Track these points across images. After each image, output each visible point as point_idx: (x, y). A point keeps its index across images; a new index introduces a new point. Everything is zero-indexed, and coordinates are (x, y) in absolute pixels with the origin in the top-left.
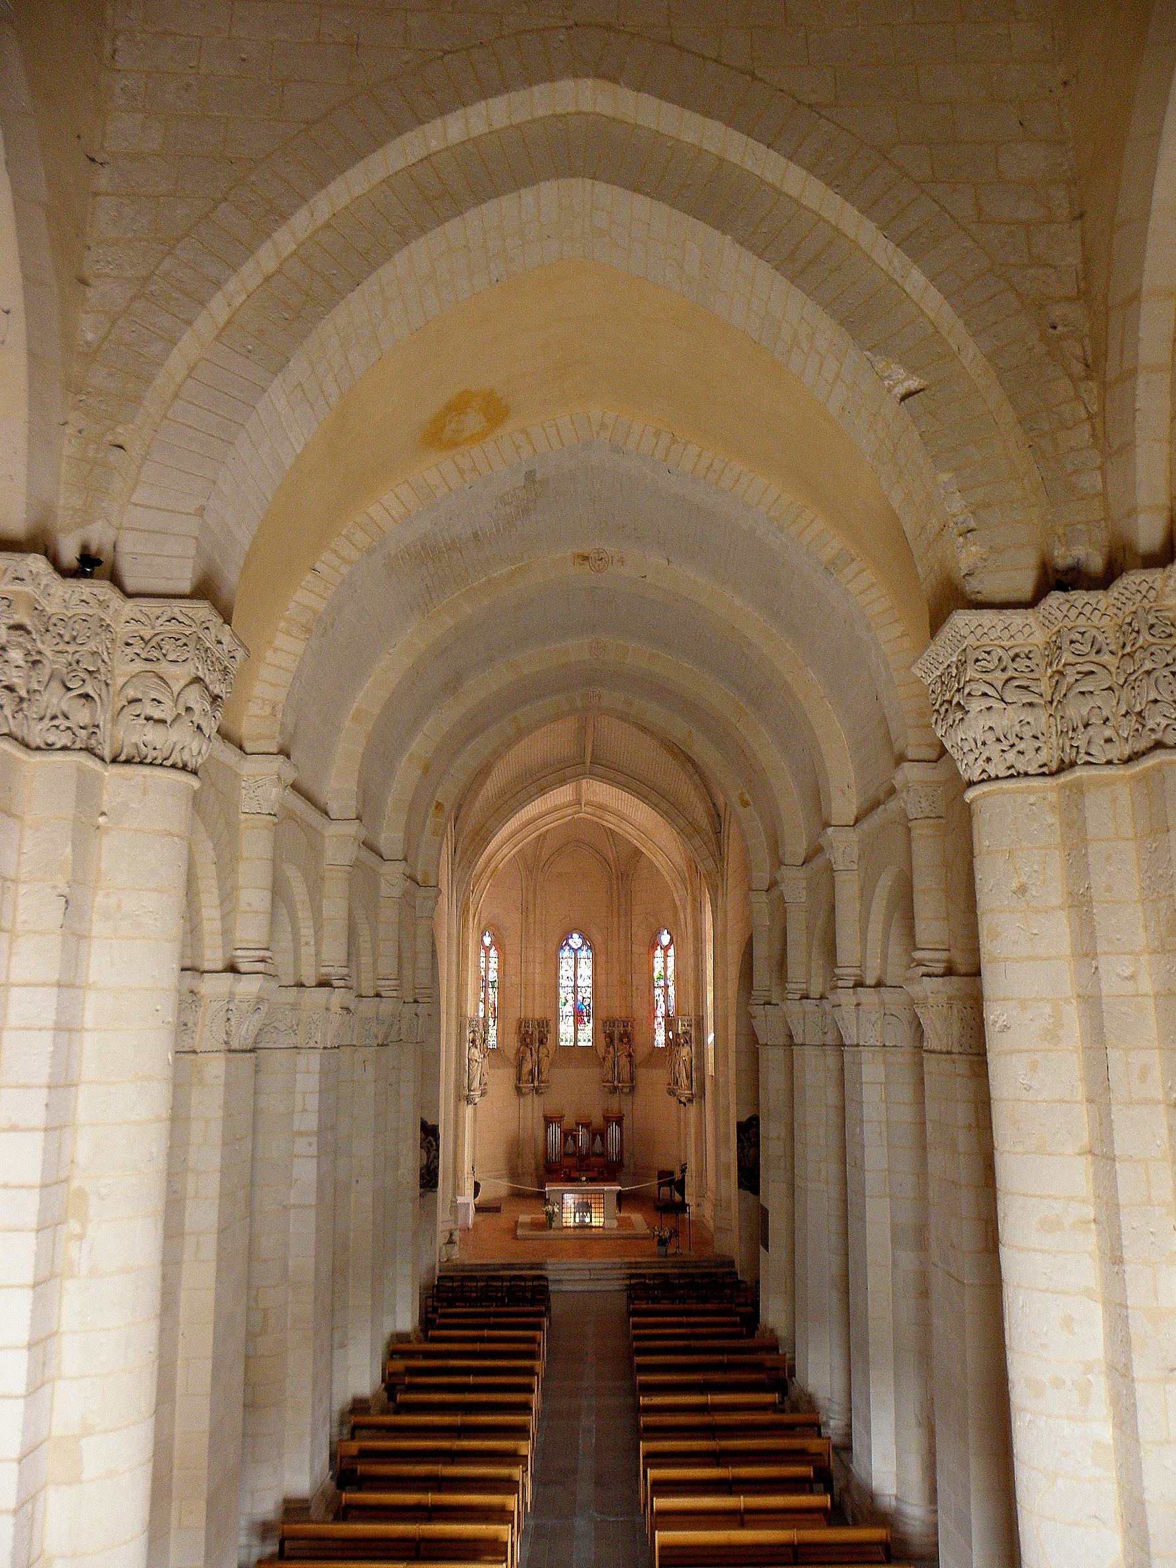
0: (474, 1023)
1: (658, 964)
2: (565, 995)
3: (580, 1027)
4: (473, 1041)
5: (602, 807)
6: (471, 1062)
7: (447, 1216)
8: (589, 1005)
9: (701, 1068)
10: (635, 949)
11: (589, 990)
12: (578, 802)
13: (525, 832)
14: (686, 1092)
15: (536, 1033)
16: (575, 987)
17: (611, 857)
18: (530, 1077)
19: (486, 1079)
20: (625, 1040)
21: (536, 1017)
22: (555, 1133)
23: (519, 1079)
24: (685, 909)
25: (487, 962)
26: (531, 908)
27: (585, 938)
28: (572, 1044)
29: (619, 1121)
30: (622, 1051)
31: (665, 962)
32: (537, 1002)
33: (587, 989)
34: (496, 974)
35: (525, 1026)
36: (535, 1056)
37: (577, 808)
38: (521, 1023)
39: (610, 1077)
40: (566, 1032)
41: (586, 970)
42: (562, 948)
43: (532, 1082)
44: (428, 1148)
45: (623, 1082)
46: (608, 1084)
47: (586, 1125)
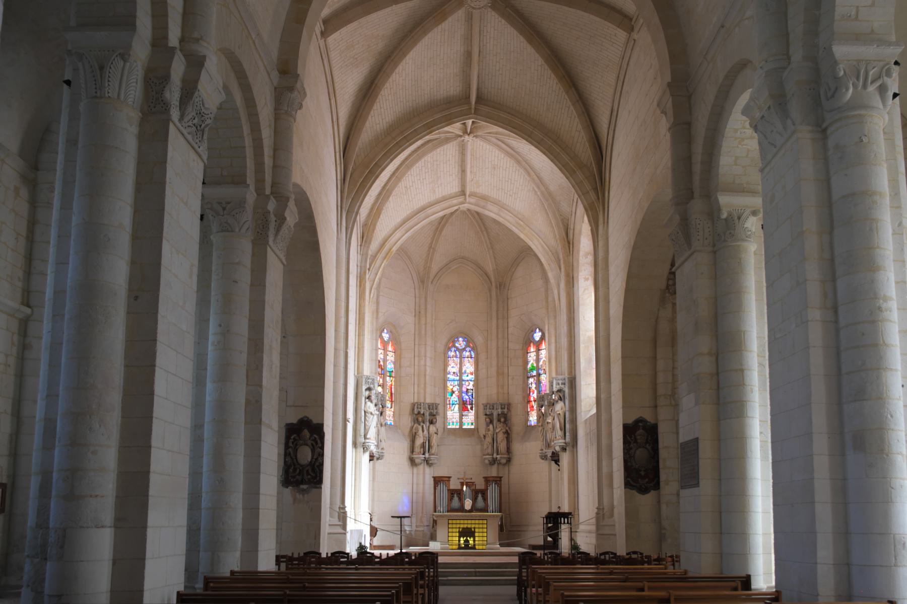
0: (370, 381)
1: (532, 357)
2: (451, 387)
3: (465, 413)
4: (369, 398)
6: (367, 414)
7: (336, 521)
8: (473, 395)
9: (574, 421)
10: (511, 346)
11: (472, 383)
13: (415, 220)
14: (560, 441)
15: (427, 414)
16: (461, 380)
17: (490, 267)
18: (422, 449)
20: (502, 420)
21: (428, 401)
22: (443, 491)
23: (412, 450)
24: (558, 285)
25: (386, 355)
26: (423, 312)
27: (469, 341)
28: (458, 427)
29: (498, 480)
30: (500, 428)
32: (429, 390)
33: (470, 382)
34: (393, 366)
35: (418, 408)
38: (414, 405)
39: (490, 451)
40: (453, 415)
41: (469, 367)
42: (449, 349)
43: (424, 454)
44: (312, 445)
45: (502, 454)
46: (487, 456)
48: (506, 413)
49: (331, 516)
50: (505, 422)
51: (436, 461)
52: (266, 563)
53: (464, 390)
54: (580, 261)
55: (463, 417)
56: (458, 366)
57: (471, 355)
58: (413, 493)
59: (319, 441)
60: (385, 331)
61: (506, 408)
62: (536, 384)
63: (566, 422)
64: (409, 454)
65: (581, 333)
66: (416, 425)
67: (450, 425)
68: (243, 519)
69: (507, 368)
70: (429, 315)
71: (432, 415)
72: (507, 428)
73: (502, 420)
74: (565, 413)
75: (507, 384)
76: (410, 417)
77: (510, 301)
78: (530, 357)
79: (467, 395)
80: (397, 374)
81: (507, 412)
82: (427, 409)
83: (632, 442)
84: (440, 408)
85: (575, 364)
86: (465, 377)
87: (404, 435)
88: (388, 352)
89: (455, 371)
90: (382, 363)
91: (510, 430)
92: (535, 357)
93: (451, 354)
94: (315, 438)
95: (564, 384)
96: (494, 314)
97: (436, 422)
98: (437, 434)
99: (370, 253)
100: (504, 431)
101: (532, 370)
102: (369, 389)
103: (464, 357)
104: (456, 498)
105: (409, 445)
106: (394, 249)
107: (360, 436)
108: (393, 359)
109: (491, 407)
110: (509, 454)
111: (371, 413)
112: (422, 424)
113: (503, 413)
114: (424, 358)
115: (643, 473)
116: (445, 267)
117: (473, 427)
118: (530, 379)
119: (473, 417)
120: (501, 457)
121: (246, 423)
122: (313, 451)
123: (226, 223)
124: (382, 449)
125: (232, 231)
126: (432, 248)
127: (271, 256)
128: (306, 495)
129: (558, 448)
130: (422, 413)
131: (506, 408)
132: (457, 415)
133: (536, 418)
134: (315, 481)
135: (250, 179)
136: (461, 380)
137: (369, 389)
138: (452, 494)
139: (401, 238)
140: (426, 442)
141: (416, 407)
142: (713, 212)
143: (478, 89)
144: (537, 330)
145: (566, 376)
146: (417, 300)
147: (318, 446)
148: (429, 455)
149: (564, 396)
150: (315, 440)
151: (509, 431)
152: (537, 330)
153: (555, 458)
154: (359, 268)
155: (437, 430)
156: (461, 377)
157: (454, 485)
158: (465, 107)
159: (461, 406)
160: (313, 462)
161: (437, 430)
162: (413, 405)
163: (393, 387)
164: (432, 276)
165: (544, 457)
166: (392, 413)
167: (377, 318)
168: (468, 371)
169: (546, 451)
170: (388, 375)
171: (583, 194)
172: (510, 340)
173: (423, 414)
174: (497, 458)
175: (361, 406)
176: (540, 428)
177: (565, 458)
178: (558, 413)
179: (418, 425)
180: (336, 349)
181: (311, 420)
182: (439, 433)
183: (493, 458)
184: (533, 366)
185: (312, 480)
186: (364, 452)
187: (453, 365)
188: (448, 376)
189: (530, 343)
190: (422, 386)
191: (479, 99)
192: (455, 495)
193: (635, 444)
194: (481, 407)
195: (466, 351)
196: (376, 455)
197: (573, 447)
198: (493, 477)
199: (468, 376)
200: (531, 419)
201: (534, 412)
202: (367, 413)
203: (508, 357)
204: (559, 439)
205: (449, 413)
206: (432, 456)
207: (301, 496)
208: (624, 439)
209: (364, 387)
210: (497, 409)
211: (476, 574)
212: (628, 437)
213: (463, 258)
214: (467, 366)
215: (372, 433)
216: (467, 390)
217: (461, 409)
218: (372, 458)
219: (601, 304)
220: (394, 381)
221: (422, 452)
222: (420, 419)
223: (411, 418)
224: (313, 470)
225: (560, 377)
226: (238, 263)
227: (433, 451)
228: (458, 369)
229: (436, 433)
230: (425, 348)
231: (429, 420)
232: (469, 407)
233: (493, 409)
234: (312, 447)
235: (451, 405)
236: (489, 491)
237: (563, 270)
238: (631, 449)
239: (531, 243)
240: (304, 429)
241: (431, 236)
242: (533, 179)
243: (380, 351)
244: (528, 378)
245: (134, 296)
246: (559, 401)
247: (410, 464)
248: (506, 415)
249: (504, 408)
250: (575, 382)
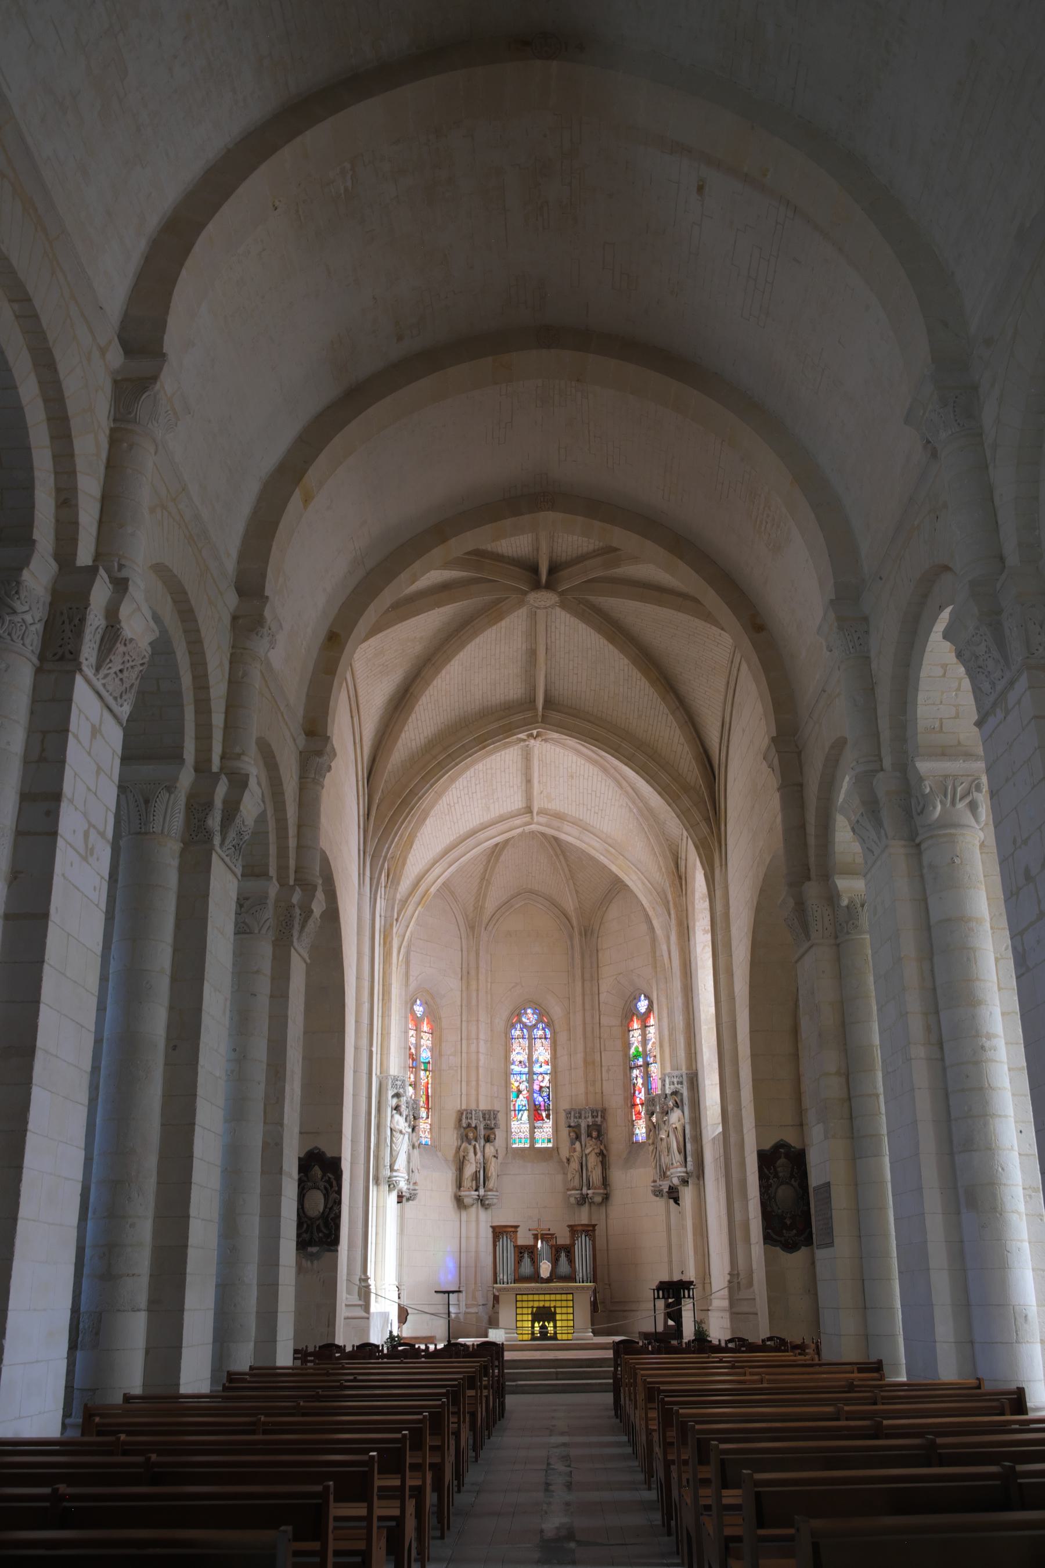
0: (399, 1083)
1: (635, 1037)
2: (517, 1084)
3: (538, 1124)
4: (397, 1108)
5: (560, 816)
6: (394, 1133)
7: (355, 1299)
8: (549, 1095)
9: (698, 1138)
10: (604, 1021)
11: (547, 1077)
12: (529, 810)
14: (679, 1169)
15: (481, 1127)
16: (531, 1073)
17: (570, 904)
18: (474, 1182)
19: (416, 1177)
20: (594, 1134)
21: (483, 1106)
22: (507, 1247)
23: (459, 1185)
24: (668, 938)
25: (419, 1038)
26: (473, 972)
27: (542, 1014)
28: (527, 1146)
30: (591, 1148)
31: (644, 1035)
32: (483, 1090)
33: (545, 1076)
34: (429, 1054)
35: (467, 1118)
36: (479, 1154)
37: (526, 818)
38: (462, 1114)
39: (576, 1182)
40: (520, 1126)
41: (543, 1053)
42: (513, 1026)
44: (326, 1188)
45: (595, 1188)
46: (573, 1192)
47: (546, 1237)
48: (599, 1123)
49: (349, 1292)
50: (598, 1137)
51: (495, 1201)
52: (284, 1358)
53: (536, 1087)
54: (696, 906)
55: (536, 1130)
56: (527, 1051)
57: (545, 1035)
58: (460, 1252)
59: (334, 1183)
60: (418, 1002)
61: (599, 1117)
62: (643, 1078)
63: (687, 1140)
64: (455, 1190)
65: (701, 1008)
66: (464, 1145)
67: (515, 1143)
68: (257, 1299)
69: (599, 1053)
70: (482, 977)
71: (487, 1127)
72: (602, 1147)
73: (594, 1134)
74: (684, 1127)
75: (600, 1078)
76: (456, 1132)
77: (600, 955)
78: (633, 1036)
79: (540, 1096)
80: (435, 1067)
81: (602, 1122)
82: (481, 1119)
83: (772, 1176)
84: (501, 1117)
85: (696, 1053)
86: (536, 1069)
87: (446, 1160)
88: (422, 1034)
89: (522, 1059)
90: (413, 1051)
91: (607, 1150)
92: (640, 1037)
93: (516, 1033)
94: (329, 1178)
95: (681, 1083)
96: (578, 973)
97: (495, 1139)
98: (497, 1158)
99: (398, 896)
100: (597, 1151)
101: (636, 1057)
102: (397, 1095)
103: (535, 1038)
104: (527, 1260)
105: (454, 1178)
106: (433, 890)
107: (385, 1166)
108: (429, 1043)
109: (577, 1115)
110: (605, 1188)
111: (401, 1132)
112: (473, 1143)
113: (595, 1124)
114: (475, 1041)
115: (788, 1222)
116: (506, 904)
117: (550, 1145)
118: (635, 1071)
119: (551, 1130)
120: (593, 1193)
121: (263, 1172)
122: (326, 1196)
123: (244, 922)
124: (415, 1184)
125: (250, 933)
126: (485, 880)
127: (295, 958)
128: (315, 1262)
129: (676, 1181)
130: (473, 1125)
131: (599, 1117)
132: (526, 1127)
133: (644, 1130)
134: (329, 1240)
135: (272, 872)
136: (531, 1073)
137: (397, 1095)
138: (521, 1253)
139: (441, 874)
140: (479, 1171)
141: (464, 1116)
142: (832, 897)
143: (546, 691)
144: (642, 997)
145: (684, 1071)
146: (465, 953)
147: (333, 1189)
148: (485, 1191)
149: (682, 1100)
150: (329, 1182)
151: (605, 1152)
152: (642, 997)
153: (674, 1195)
154: (383, 918)
155: (497, 1151)
156: (531, 1068)
157: (524, 1238)
158: (530, 714)
159: (532, 1112)
160: (326, 1214)
161: (497, 1151)
162: (460, 1113)
163: (430, 1086)
164: (485, 921)
165: (658, 1193)
166: (429, 1127)
167: (407, 985)
168: (541, 1059)
169: (661, 1183)
170: (423, 1068)
171: (690, 825)
172: (602, 1012)
173: (476, 1128)
174: (587, 1194)
175: (386, 1120)
176: (651, 1148)
177: (687, 1195)
178: (674, 1126)
179: (467, 1145)
180: (356, 1048)
181: (323, 1153)
182: (500, 1157)
183: (582, 1194)
184: (638, 1051)
185: (324, 1240)
186: (390, 1190)
187: (518, 1049)
188: (512, 1067)
189: (633, 1014)
190: (474, 1083)
191: (549, 702)
192: (526, 1255)
193: (775, 1179)
194: (562, 1116)
195: (538, 1029)
196: (406, 1194)
197: (698, 1178)
198: (582, 1225)
199: (541, 1066)
200: (637, 1131)
201: (642, 1121)
202: (395, 1131)
203: (600, 1038)
204: (677, 1168)
205: (514, 1125)
206: (489, 1193)
207: (309, 1263)
208: (759, 1171)
209: (390, 1093)
210: (585, 1118)
211: (557, 1376)
212: (766, 1170)
213: (532, 892)
214: (539, 1051)
215: (401, 1163)
216: (541, 1087)
217: (532, 1117)
218: (400, 1198)
219: (722, 977)
220: (432, 1077)
221: (474, 1188)
222: (471, 1135)
223: (457, 1134)
224: (327, 1225)
225: (676, 1073)
226: (257, 972)
227: (491, 1184)
228: (526, 1057)
229: (495, 1156)
230: (478, 1028)
231: (484, 1136)
232: (544, 1114)
233: (580, 1117)
234: (324, 1192)
236: (576, 1246)
237: (673, 916)
238: (771, 1185)
239: (626, 877)
240: (314, 1166)
241: (484, 864)
242: (627, 792)
243: (412, 1033)
244: (631, 1068)
245: (172, 1047)
246: (675, 1109)
247: (456, 1206)
248: (600, 1126)
249: (597, 1117)
250: (697, 1080)
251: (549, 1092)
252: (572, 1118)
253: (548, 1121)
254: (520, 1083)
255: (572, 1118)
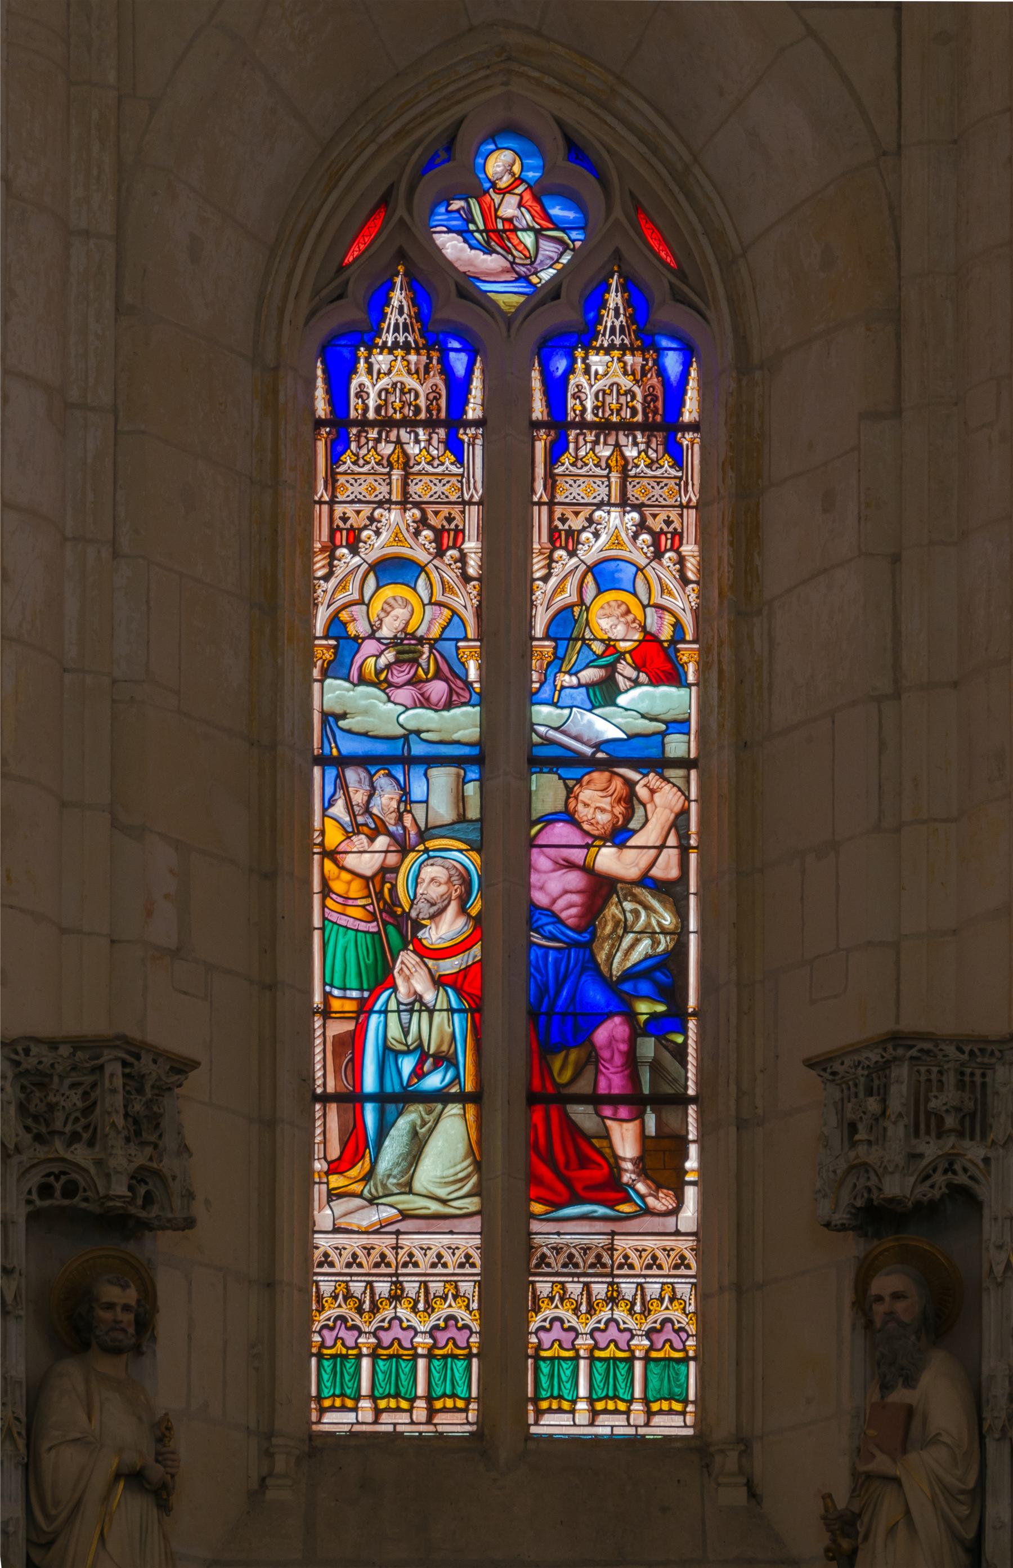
235: (370, 1114)
251: (681, 934)
252: (897, 1131)
253: (661, 1202)
254: (403, 849)
255: (897, 1131)
